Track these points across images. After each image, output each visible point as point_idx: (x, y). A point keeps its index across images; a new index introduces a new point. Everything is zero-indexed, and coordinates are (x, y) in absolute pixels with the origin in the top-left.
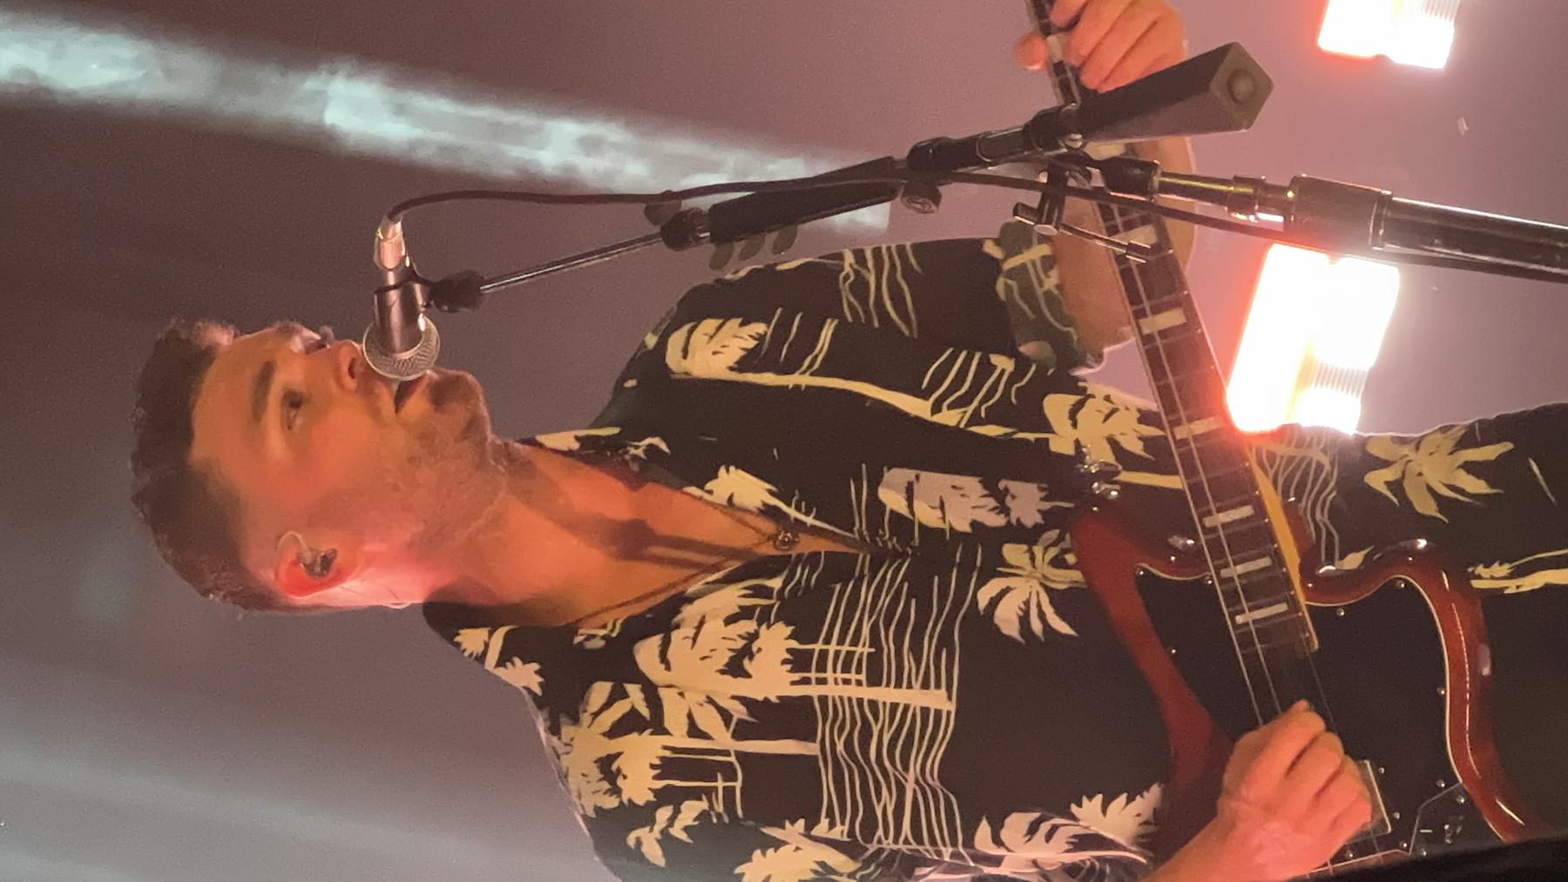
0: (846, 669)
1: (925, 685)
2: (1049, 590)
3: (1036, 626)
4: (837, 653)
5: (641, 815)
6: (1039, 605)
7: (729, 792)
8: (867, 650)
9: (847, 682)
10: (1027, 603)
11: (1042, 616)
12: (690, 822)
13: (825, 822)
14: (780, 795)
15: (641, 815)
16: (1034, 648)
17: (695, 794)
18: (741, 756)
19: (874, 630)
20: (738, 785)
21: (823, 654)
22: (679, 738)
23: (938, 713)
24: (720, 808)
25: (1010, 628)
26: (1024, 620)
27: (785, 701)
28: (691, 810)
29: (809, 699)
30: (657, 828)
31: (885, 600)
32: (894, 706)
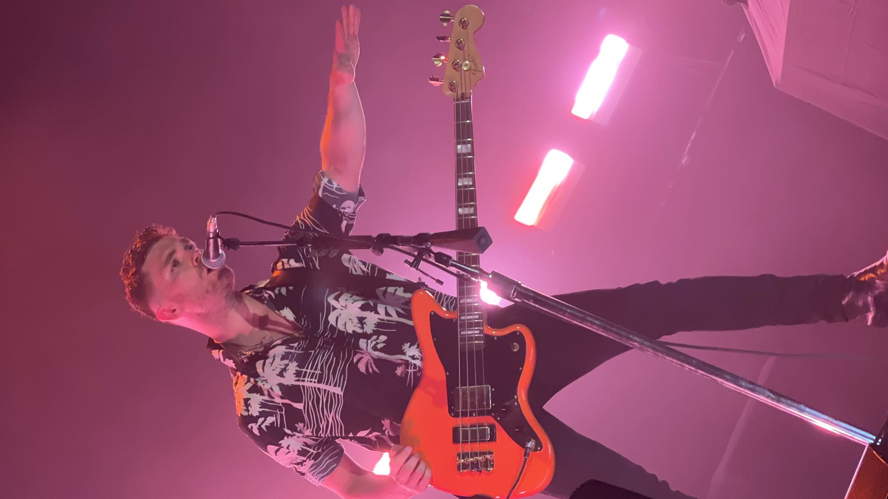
3: (371, 370)
14: (293, 418)
15: (254, 419)
16: (368, 376)
17: (271, 414)
22: (266, 398)
27: (293, 386)
28: (270, 420)
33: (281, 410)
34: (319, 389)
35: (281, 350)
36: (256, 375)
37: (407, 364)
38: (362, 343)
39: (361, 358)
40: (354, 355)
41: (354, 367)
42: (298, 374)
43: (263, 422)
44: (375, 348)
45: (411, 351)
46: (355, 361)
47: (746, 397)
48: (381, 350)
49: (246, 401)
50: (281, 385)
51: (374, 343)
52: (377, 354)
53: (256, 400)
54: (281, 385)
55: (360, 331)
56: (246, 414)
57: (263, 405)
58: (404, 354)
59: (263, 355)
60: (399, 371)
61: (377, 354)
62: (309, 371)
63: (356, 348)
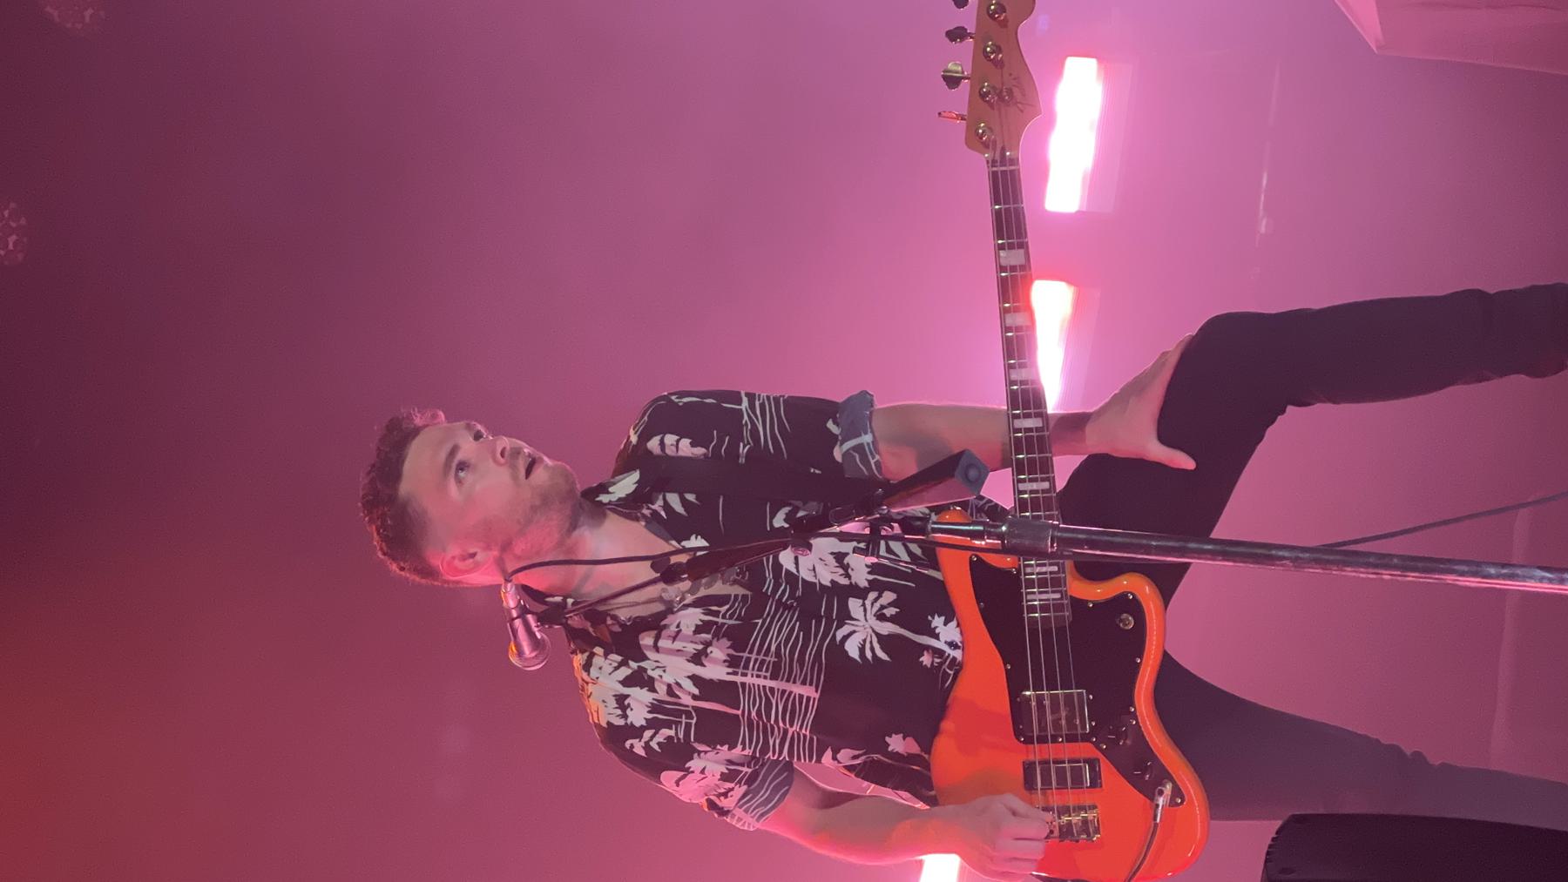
0: (760, 669)
1: (804, 683)
2: (877, 634)
3: (869, 655)
5: (637, 732)
11: (872, 649)
13: (740, 747)
14: (717, 730)
15: (637, 732)
17: (668, 725)
18: (696, 709)
19: (778, 647)
21: (748, 660)
23: (808, 699)
25: (854, 653)
26: (862, 650)
27: (721, 682)
28: (666, 732)
31: (785, 631)
32: (784, 692)
33: (689, 716)
34: (772, 689)
35: (691, 618)
36: (645, 658)
37: (939, 653)
38: (854, 605)
40: (839, 627)
41: (838, 649)
42: (733, 662)
43: (652, 738)
44: (881, 617)
45: (947, 632)
46: (839, 638)
47: (1503, 593)
48: (892, 619)
49: (621, 700)
50: (694, 679)
51: (877, 605)
52: (887, 628)
53: (640, 698)
54: (694, 679)
55: (844, 581)
56: (621, 722)
57: (655, 707)
58: (937, 637)
59: (655, 624)
60: (926, 659)
61: (887, 628)
62: (754, 656)
63: (845, 616)
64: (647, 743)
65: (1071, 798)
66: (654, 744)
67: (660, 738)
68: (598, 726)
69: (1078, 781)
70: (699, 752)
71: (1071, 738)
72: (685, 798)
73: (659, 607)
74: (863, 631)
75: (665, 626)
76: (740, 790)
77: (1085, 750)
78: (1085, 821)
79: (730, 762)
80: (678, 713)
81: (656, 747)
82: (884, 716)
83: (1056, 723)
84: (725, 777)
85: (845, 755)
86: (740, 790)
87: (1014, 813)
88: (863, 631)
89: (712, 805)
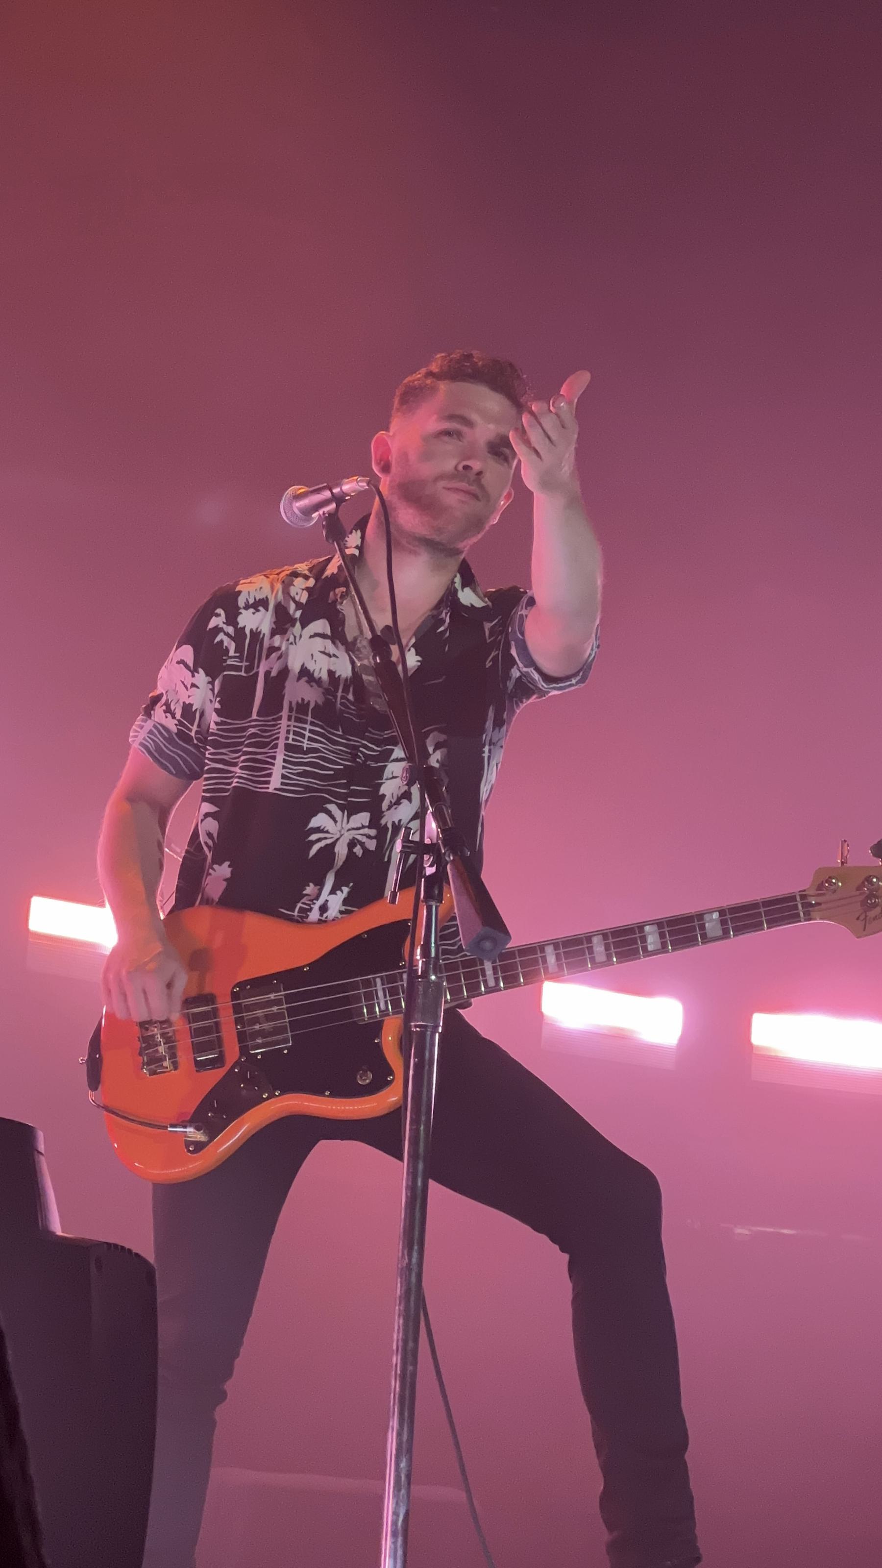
1: (283, 776)
2: (333, 844)
3: (313, 837)
4: (305, 729)
5: (232, 619)
6: (326, 838)
7: (238, 669)
8: (305, 746)
9: (288, 732)
10: (327, 832)
11: (319, 840)
12: (225, 644)
13: (218, 719)
18: (257, 674)
19: (316, 750)
20: (243, 674)
21: (305, 722)
23: (268, 782)
24: (229, 662)
25: (314, 822)
26: (318, 830)
29: (281, 709)
30: (225, 626)
33: (248, 669)
39: (336, 822)
40: (341, 808)
41: (319, 807)
42: (302, 708)
49: (260, 604)
52: (341, 851)
61: (341, 851)
62: (308, 727)
64: (221, 630)
65: (184, 1044)
66: (221, 637)
67: (227, 641)
68: (237, 584)
69: (199, 1048)
70: (212, 683)
71: (242, 1037)
72: (163, 673)
73: (350, 635)
74: (337, 829)
75: (334, 643)
76: (171, 724)
77: (232, 1052)
78: (162, 1059)
79: (202, 715)
80: (251, 658)
81: (218, 639)
82: (260, 852)
83: (256, 1020)
84: (187, 710)
85: (212, 825)
86: (171, 724)
87: (169, 986)
88: (337, 829)
89: (156, 700)
